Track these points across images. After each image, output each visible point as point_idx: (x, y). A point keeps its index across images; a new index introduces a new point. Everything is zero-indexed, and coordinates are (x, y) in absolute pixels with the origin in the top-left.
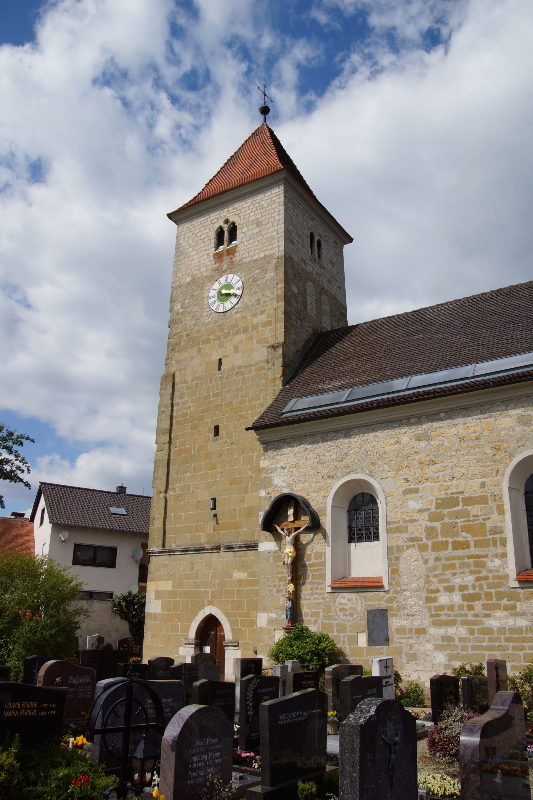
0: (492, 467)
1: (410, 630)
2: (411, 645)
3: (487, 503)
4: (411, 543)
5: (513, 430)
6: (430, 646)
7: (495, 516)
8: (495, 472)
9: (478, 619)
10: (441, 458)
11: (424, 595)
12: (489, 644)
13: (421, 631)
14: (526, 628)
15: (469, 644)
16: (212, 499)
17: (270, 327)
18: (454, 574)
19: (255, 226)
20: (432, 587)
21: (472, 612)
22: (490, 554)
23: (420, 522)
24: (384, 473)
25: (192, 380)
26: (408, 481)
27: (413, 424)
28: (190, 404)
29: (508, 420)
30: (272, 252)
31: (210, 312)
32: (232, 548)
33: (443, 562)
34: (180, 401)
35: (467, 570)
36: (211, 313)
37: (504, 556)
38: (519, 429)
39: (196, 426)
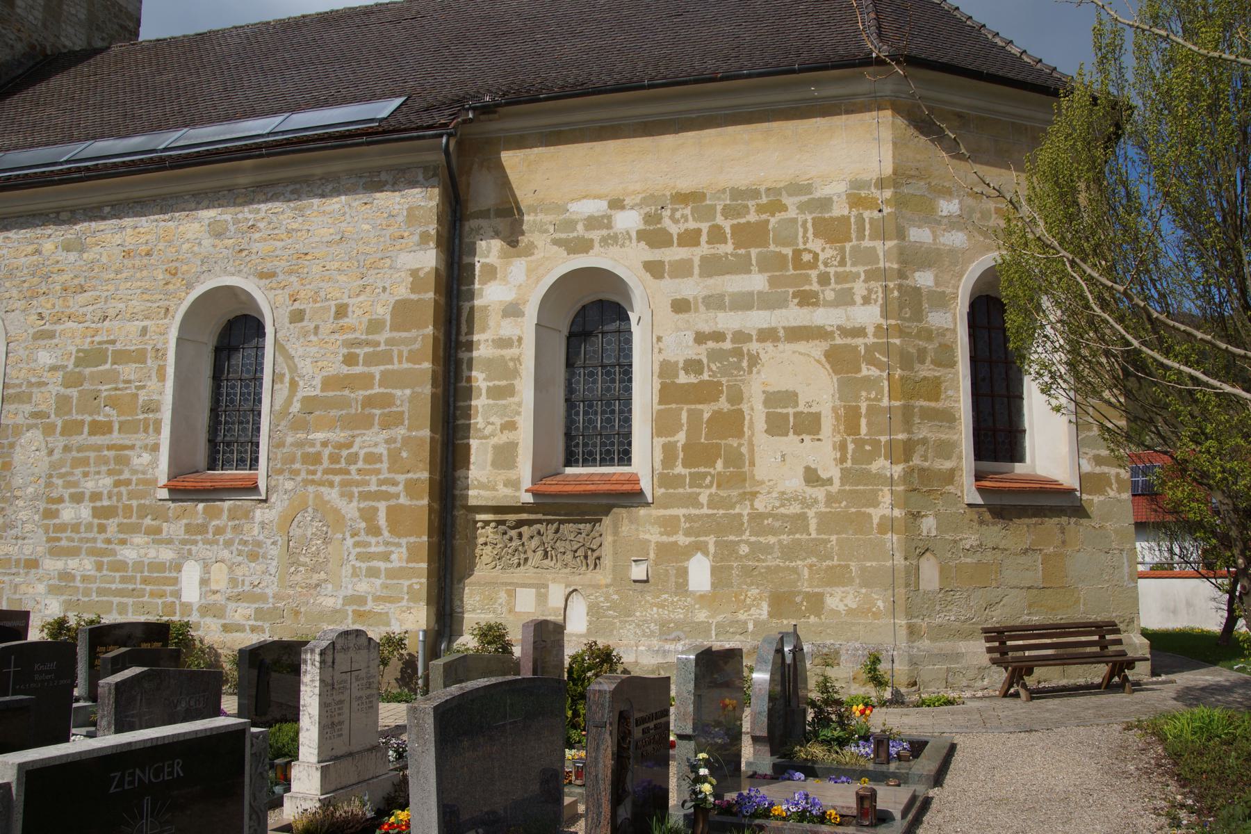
0: (161, 303)
1: (18, 562)
2: (16, 586)
3: (145, 362)
4: (34, 421)
5: (200, 244)
6: (41, 588)
7: (153, 384)
8: (163, 311)
9: (110, 547)
10: (94, 282)
11: (42, 506)
12: (121, 586)
13: (32, 564)
14: (171, 563)
15: (94, 586)
18: (86, 475)
20: (54, 495)
21: (103, 536)
22: (138, 444)
23: (50, 387)
24: (11, 302)
26: (42, 318)
27: (63, 222)
29: (196, 225)
33: (74, 454)
35: (104, 468)
37: (155, 448)
38: (207, 242)
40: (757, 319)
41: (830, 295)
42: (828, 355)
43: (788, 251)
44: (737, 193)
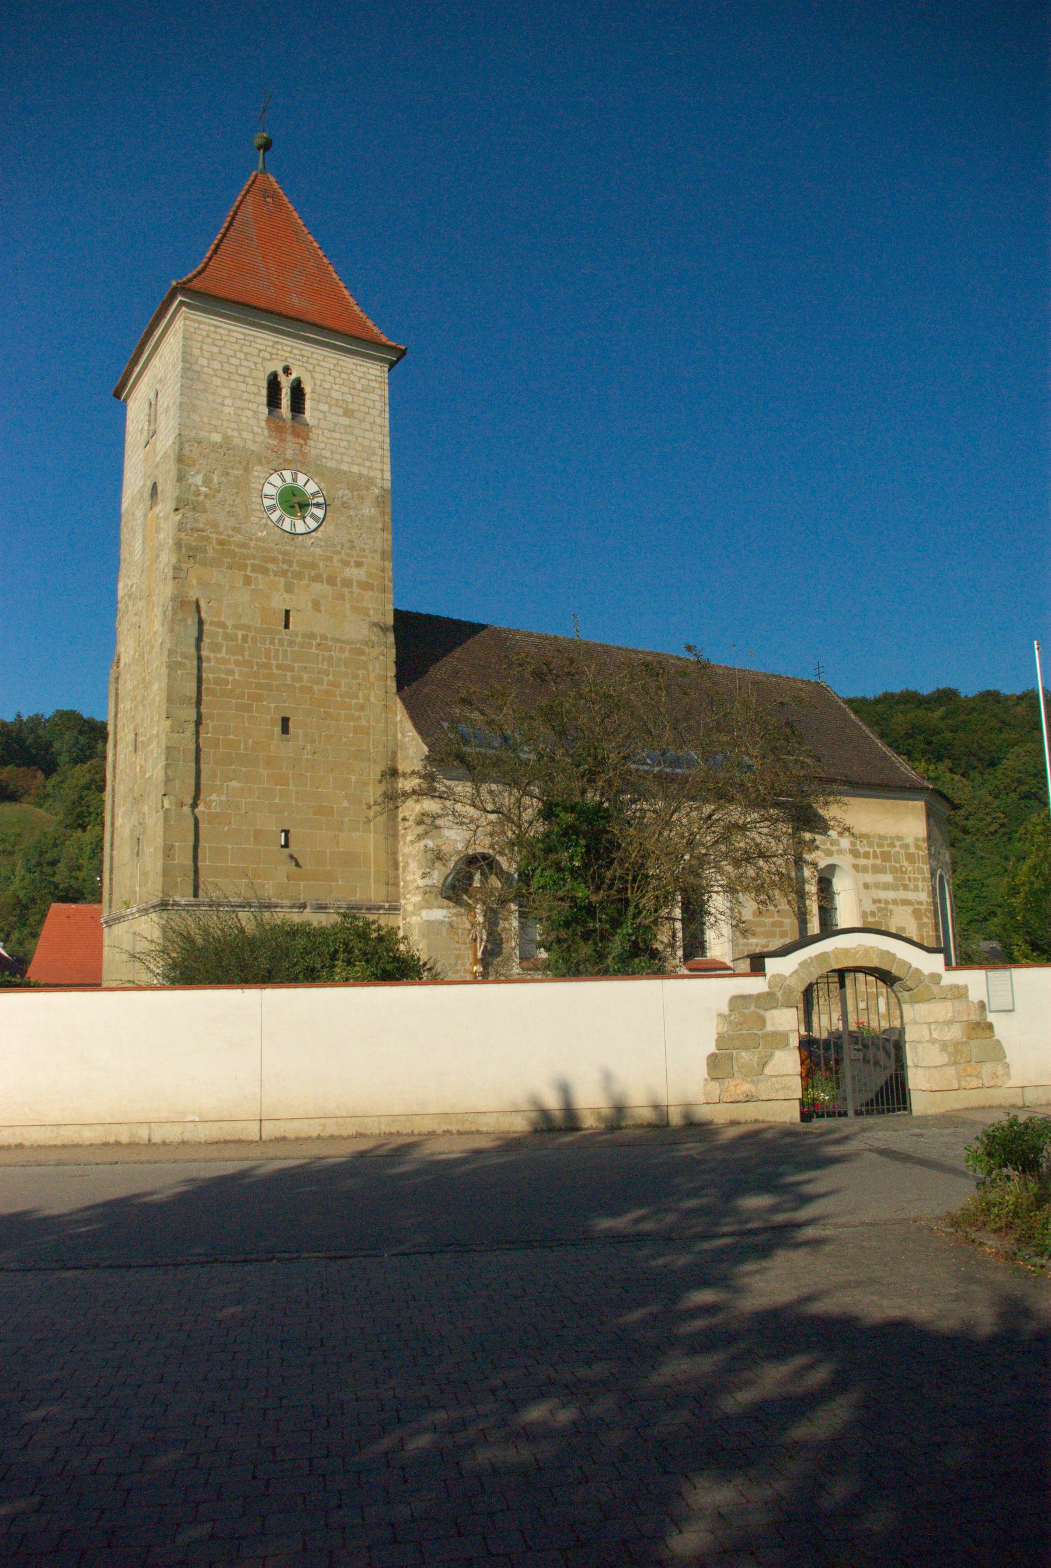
16: (283, 831)
17: (370, 593)
19: (341, 411)
25: (236, 627)
28: (232, 666)
30: (372, 474)
31: (264, 521)
32: (326, 908)
34: (212, 655)
36: (266, 524)
39: (248, 708)
40: (890, 895)
41: (912, 887)
42: (914, 912)
43: (898, 865)
44: (882, 837)
